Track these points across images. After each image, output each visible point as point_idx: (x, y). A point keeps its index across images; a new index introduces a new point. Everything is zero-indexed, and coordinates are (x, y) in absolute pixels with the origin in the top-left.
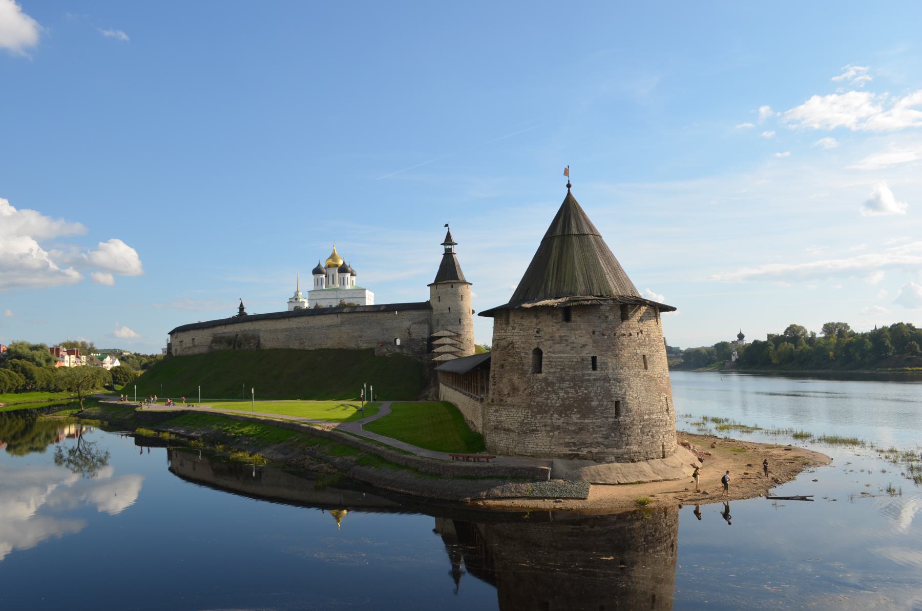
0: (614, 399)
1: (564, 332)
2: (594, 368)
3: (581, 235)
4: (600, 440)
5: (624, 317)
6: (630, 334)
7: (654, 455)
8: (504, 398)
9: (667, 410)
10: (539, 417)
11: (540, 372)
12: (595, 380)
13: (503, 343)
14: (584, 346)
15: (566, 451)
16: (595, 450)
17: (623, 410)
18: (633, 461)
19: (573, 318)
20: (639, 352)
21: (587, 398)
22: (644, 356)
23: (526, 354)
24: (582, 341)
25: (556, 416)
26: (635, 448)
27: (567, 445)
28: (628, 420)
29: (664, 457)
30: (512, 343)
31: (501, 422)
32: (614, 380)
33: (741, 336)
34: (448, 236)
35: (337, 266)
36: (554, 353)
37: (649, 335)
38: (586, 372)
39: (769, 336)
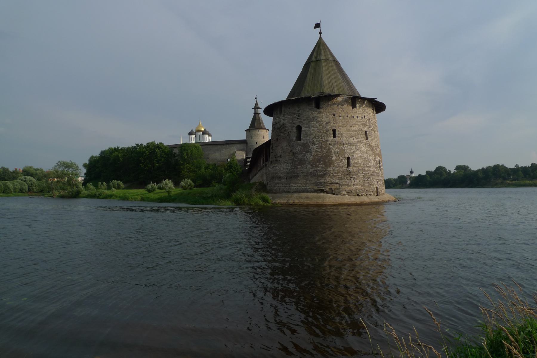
0: (347, 156)
1: (315, 114)
2: (334, 136)
3: (327, 60)
4: (337, 181)
5: (354, 106)
6: (357, 117)
7: (371, 193)
8: (278, 159)
9: (380, 167)
10: (299, 167)
11: (301, 140)
12: (334, 144)
13: (278, 126)
14: (327, 123)
15: (316, 188)
16: (333, 188)
17: (352, 163)
18: (358, 195)
19: (321, 106)
20: (362, 128)
21: (329, 155)
22: (366, 132)
23: (292, 129)
24: (327, 120)
25: (309, 166)
26: (359, 187)
27: (316, 184)
28: (355, 169)
29: (377, 195)
30: (283, 124)
31: (276, 173)
32: (347, 144)
33: (412, 172)
34: (257, 104)
35: (201, 131)
36: (309, 128)
37: (369, 120)
38: (329, 139)
39: (427, 172)
